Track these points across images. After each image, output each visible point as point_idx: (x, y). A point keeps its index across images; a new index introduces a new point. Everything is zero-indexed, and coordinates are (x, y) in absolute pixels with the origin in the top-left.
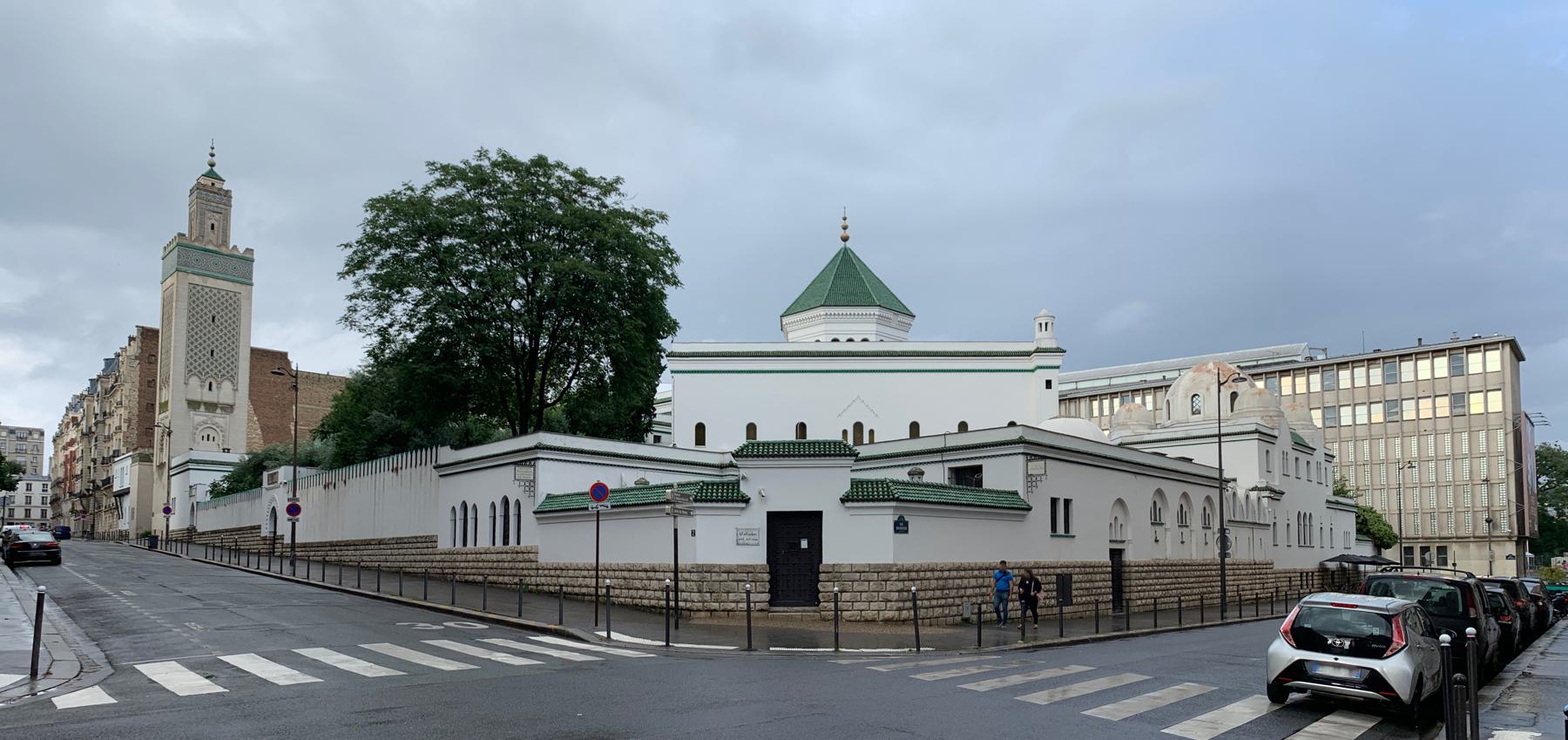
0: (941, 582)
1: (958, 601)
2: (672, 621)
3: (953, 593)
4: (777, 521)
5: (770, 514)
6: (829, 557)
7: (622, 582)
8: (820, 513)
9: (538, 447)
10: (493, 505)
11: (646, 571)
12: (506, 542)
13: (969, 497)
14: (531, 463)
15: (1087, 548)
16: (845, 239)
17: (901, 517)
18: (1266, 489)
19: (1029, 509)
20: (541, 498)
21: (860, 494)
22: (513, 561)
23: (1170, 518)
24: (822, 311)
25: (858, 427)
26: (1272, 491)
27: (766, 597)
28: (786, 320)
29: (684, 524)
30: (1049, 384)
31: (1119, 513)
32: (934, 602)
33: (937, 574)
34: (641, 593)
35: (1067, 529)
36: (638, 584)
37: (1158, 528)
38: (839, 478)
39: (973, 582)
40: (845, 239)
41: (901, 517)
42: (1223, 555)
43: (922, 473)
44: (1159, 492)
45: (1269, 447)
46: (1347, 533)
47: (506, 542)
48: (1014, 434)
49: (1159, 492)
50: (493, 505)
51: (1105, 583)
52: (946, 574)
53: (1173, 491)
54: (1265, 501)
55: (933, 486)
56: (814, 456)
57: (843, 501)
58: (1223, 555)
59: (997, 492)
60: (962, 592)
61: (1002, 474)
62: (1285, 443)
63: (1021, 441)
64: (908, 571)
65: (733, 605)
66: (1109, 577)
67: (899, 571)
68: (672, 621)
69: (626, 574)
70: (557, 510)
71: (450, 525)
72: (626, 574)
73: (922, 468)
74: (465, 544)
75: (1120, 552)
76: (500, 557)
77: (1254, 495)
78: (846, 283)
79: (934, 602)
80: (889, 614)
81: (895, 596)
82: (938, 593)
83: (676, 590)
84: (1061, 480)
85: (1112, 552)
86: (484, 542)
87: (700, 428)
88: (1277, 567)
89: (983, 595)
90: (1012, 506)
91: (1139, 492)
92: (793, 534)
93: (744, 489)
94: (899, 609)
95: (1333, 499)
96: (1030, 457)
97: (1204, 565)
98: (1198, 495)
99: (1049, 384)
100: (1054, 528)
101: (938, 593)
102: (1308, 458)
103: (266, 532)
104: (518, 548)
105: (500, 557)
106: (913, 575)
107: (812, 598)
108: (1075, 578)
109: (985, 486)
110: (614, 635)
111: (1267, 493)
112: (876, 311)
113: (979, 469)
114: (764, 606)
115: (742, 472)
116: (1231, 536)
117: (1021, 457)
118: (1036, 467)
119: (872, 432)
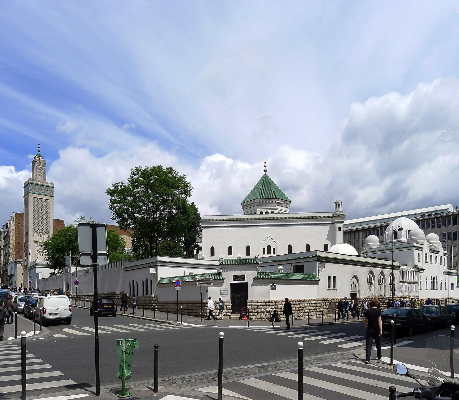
14: (155, 267)
15: (343, 292)
25: (269, 247)
31: (354, 280)
35: (334, 287)
36: (190, 308)
39: (298, 306)
53: (376, 271)
75: (356, 294)
87: (212, 249)
95: (447, 271)
100: (329, 287)
106: (277, 303)
110: (183, 323)
119: (274, 249)
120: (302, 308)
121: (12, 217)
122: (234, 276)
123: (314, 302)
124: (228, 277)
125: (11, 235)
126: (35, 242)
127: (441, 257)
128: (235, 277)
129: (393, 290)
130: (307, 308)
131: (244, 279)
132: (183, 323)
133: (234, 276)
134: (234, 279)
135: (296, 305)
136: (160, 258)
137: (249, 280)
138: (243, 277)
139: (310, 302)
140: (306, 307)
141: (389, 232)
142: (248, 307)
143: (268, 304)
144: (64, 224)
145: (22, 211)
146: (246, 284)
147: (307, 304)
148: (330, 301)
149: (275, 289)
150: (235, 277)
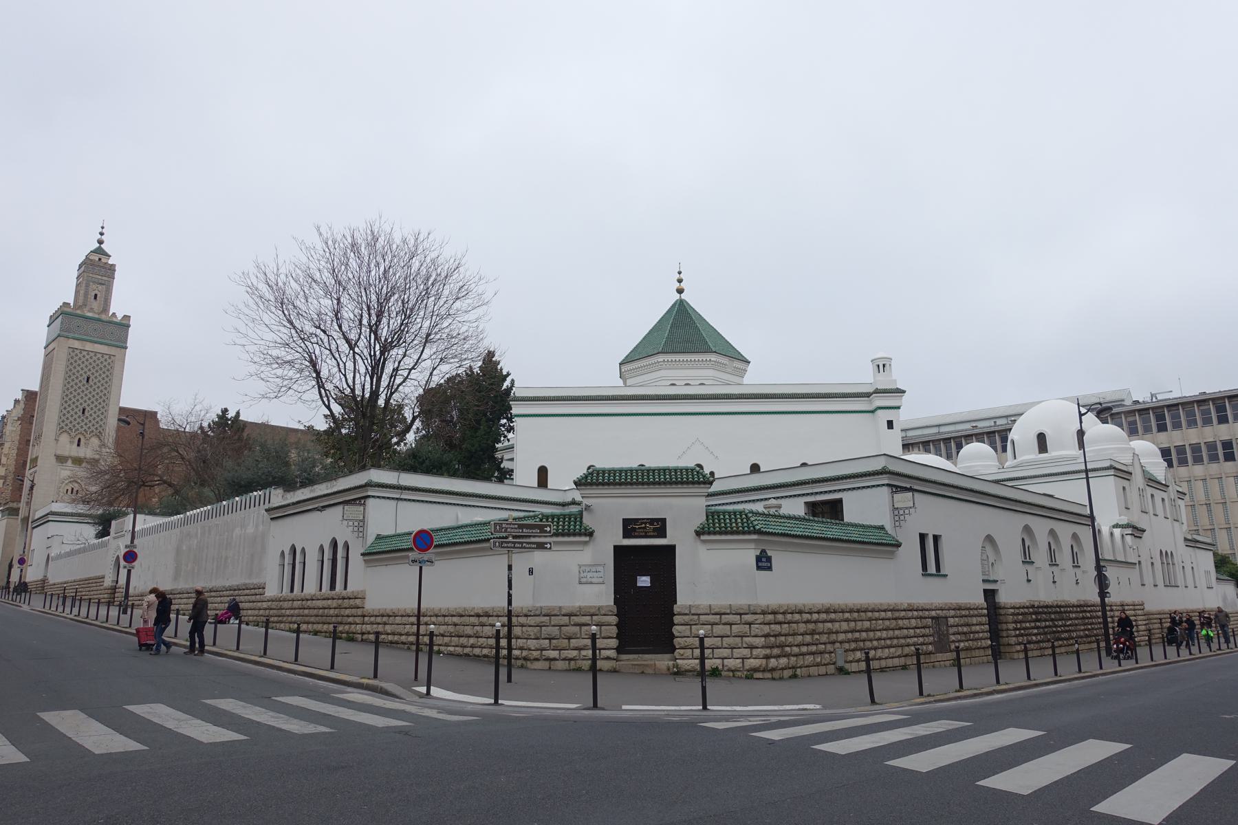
0: (811, 626)
1: (829, 647)
2: (503, 672)
3: (824, 638)
6: (684, 598)
7: (451, 629)
9: (369, 485)
10: (322, 549)
11: (478, 616)
12: (333, 587)
13: (834, 531)
14: (361, 501)
15: (961, 588)
16: (680, 291)
17: (763, 551)
18: (1128, 526)
19: (898, 545)
20: (371, 539)
21: (718, 526)
22: (339, 607)
23: (1040, 556)
24: (661, 358)
26: (1134, 528)
27: (614, 643)
29: (522, 561)
30: (890, 424)
31: (989, 548)
32: (804, 649)
34: (472, 641)
36: (468, 630)
37: (1028, 567)
39: (845, 626)
40: (680, 291)
41: (763, 551)
42: (1103, 594)
43: (780, 507)
44: (1027, 529)
45: (1125, 483)
46: (1207, 573)
47: (333, 587)
48: (877, 465)
49: (1027, 529)
50: (322, 549)
51: (981, 626)
52: (815, 616)
53: (1041, 527)
54: (1128, 538)
55: (789, 518)
56: (664, 483)
58: (1103, 594)
59: (863, 526)
60: (833, 637)
61: (863, 508)
62: (1138, 480)
63: (883, 472)
64: (774, 613)
65: (575, 653)
66: (985, 620)
67: (764, 613)
68: (503, 672)
69: (455, 619)
70: (383, 552)
72: (455, 619)
76: (326, 603)
77: (1117, 532)
78: (682, 332)
79: (804, 649)
81: (760, 641)
82: (808, 638)
83: (509, 637)
84: (928, 515)
85: (985, 591)
86: (311, 588)
87: (543, 472)
89: (856, 640)
91: (1007, 527)
92: (644, 574)
93: (588, 520)
94: (767, 657)
96: (896, 489)
97: (1082, 607)
98: (1065, 531)
99: (890, 424)
100: (925, 567)
101: (808, 638)
102: (1164, 495)
103: (108, 582)
105: (326, 603)
106: (780, 617)
107: (666, 644)
108: (951, 621)
111: (1129, 531)
112: (713, 357)
113: (840, 501)
114: (612, 653)
115: (586, 502)
116: (1110, 572)
117: (885, 488)
118: (903, 499)
120: (857, 635)
121: (17, 401)
122: (626, 522)
123: (889, 614)
124: (609, 513)
125: (7, 445)
126: (61, 459)
128: (630, 527)
130: (871, 634)
131: (662, 532)
132: (435, 691)
133: (626, 522)
134: (627, 534)
135: (837, 625)
136: (377, 475)
137: (679, 536)
138: (659, 526)
139: (877, 614)
140: (867, 630)
141: (1022, 434)
142: (676, 630)
144: (157, 421)
145: (35, 387)
146: (671, 549)
147: (870, 620)
148: (933, 613)
149: (770, 568)
150: (630, 527)
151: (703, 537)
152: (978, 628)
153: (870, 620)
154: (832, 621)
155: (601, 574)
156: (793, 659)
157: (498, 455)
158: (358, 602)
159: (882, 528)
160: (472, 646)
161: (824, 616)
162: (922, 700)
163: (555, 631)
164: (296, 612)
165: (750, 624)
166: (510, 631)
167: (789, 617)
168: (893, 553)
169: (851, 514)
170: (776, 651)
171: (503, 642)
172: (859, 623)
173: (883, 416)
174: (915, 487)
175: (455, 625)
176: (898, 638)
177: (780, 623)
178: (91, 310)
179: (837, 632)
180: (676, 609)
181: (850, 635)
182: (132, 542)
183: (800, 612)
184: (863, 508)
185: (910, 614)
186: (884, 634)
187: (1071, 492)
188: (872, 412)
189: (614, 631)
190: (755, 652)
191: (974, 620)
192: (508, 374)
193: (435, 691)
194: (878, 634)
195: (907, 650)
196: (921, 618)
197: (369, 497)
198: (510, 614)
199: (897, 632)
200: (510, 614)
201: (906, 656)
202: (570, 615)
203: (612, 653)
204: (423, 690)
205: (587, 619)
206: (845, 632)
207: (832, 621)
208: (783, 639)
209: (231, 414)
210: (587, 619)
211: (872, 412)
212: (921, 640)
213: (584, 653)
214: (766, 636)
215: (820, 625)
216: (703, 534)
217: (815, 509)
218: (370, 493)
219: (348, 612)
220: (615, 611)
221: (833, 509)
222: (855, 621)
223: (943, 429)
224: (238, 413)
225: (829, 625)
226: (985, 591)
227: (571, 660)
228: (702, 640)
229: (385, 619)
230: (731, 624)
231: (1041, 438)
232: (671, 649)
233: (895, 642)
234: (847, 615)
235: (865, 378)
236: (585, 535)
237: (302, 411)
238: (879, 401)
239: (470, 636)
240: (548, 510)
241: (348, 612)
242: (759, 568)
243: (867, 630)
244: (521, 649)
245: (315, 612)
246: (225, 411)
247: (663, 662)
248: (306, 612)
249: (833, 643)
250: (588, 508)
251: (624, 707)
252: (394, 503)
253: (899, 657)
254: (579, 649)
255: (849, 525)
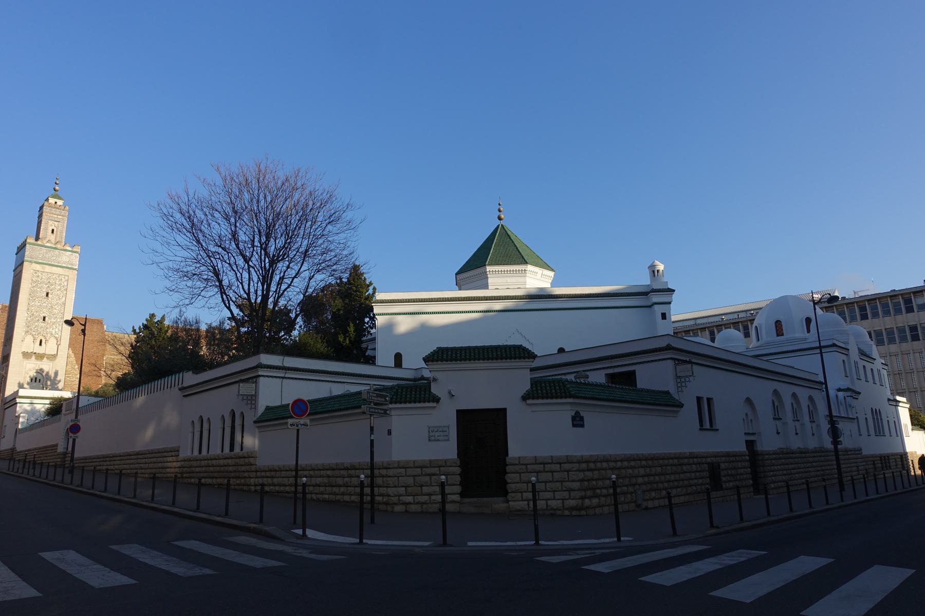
1: (631, 489)
4: (463, 416)
5: (459, 412)
6: (515, 450)
7: (326, 480)
8: (505, 410)
9: (261, 366)
11: (347, 469)
15: (728, 440)
17: (577, 413)
19: (681, 406)
20: (261, 409)
22: (236, 465)
27: (458, 489)
28: (459, 277)
33: (612, 464)
36: (340, 481)
38: (519, 378)
39: (642, 471)
41: (577, 413)
42: (836, 442)
43: (587, 377)
44: (776, 392)
48: (663, 343)
49: (776, 392)
52: (619, 464)
53: (786, 391)
57: (525, 398)
58: (836, 442)
59: (653, 391)
62: (854, 354)
63: (669, 348)
64: (587, 462)
65: (426, 498)
66: (747, 464)
69: (329, 473)
71: (190, 435)
72: (329, 473)
73: (588, 373)
74: (200, 452)
80: (572, 503)
81: (576, 485)
83: (372, 486)
84: (704, 382)
85: (747, 441)
86: (216, 451)
87: (398, 358)
88: (865, 452)
90: (664, 402)
91: (761, 391)
92: (482, 431)
93: (434, 389)
94: (583, 498)
97: (821, 451)
98: (803, 394)
103: (60, 449)
104: (241, 454)
106: (592, 465)
107: (502, 490)
108: (723, 466)
109: (640, 385)
111: (849, 394)
113: (633, 373)
116: (841, 426)
117: (671, 363)
118: (683, 369)
120: (652, 478)
123: (676, 461)
127: (879, 371)
129: (835, 433)
139: (666, 462)
140: (659, 474)
142: (509, 477)
143: (567, 466)
147: (661, 466)
148: (709, 460)
149: (582, 426)
151: (529, 402)
152: (742, 471)
153: (661, 466)
154: (632, 468)
155: (446, 433)
156: (603, 499)
157: (364, 345)
158: (251, 460)
159: (667, 393)
160: (343, 494)
161: (625, 464)
162: (714, 531)
163: (410, 481)
164: (203, 469)
165: (568, 471)
166: (372, 481)
167: (599, 465)
168: (678, 412)
169: (642, 382)
170: (589, 493)
171: (367, 490)
172: (653, 470)
173: (659, 309)
174: (694, 361)
175: (329, 477)
176: (683, 480)
177: (592, 470)
178: (49, 241)
179: (637, 477)
180: (508, 460)
181: (646, 479)
182: (76, 417)
183: (607, 461)
184: (652, 376)
185: (691, 461)
186: (672, 477)
187: (809, 364)
188: (650, 306)
189: (458, 478)
190: (572, 494)
191: (740, 464)
192: (371, 284)
193: (310, 533)
194: (668, 477)
195: (690, 490)
196: (700, 464)
197: (260, 376)
198: (372, 467)
199: (682, 476)
200: (372, 467)
201: (689, 494)
202: (421, 467)
203: (456, 498)
204: (300, 532)
205: (436, 470)
206: (642, 476)
207: (632, 468)
208: (594, 483)
209: (157, 319)
210: (436, 470)
211: (650, 306)
212: (700, 481)
213: (433, 497)
214: (581, 481)
215: (623, 471)
216: (529, 399)
217: (612, 377)
218: (260, 373)
219: (243, 468)
220: (459, 463)
221: (629, 378)
222: (650, 467)
223: (699, 322)
224: (163, 318)
225: (630, 471)
226: (747, 441)
227: (423, 503)
228: (534, 485)
229: (273, 473)
230: (552, 472)
231: (778, 324)
232: (505, 493)
233: (681, 483)
234: (644, 463)
235: (643, 280)
236: (433, 402)
237: (210, 313)
238: (655, 298)
239: (340, 486)
240: (404, 382)
241: (243, 468)
242: (574, 425)
243: (659, 474)
244: (382, 495)
245: (218, 469)
246: (152, 316)
247: (498, 504)
248: (211, 469)
249: (634, 485)
250: (435, 380)
251: (470, 544)
252: (279, 380)
253: (684, 495)
254: (430, 495)
255: (643, 390)
